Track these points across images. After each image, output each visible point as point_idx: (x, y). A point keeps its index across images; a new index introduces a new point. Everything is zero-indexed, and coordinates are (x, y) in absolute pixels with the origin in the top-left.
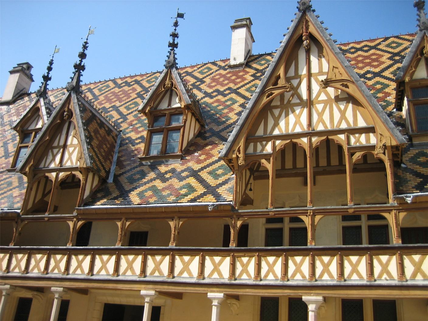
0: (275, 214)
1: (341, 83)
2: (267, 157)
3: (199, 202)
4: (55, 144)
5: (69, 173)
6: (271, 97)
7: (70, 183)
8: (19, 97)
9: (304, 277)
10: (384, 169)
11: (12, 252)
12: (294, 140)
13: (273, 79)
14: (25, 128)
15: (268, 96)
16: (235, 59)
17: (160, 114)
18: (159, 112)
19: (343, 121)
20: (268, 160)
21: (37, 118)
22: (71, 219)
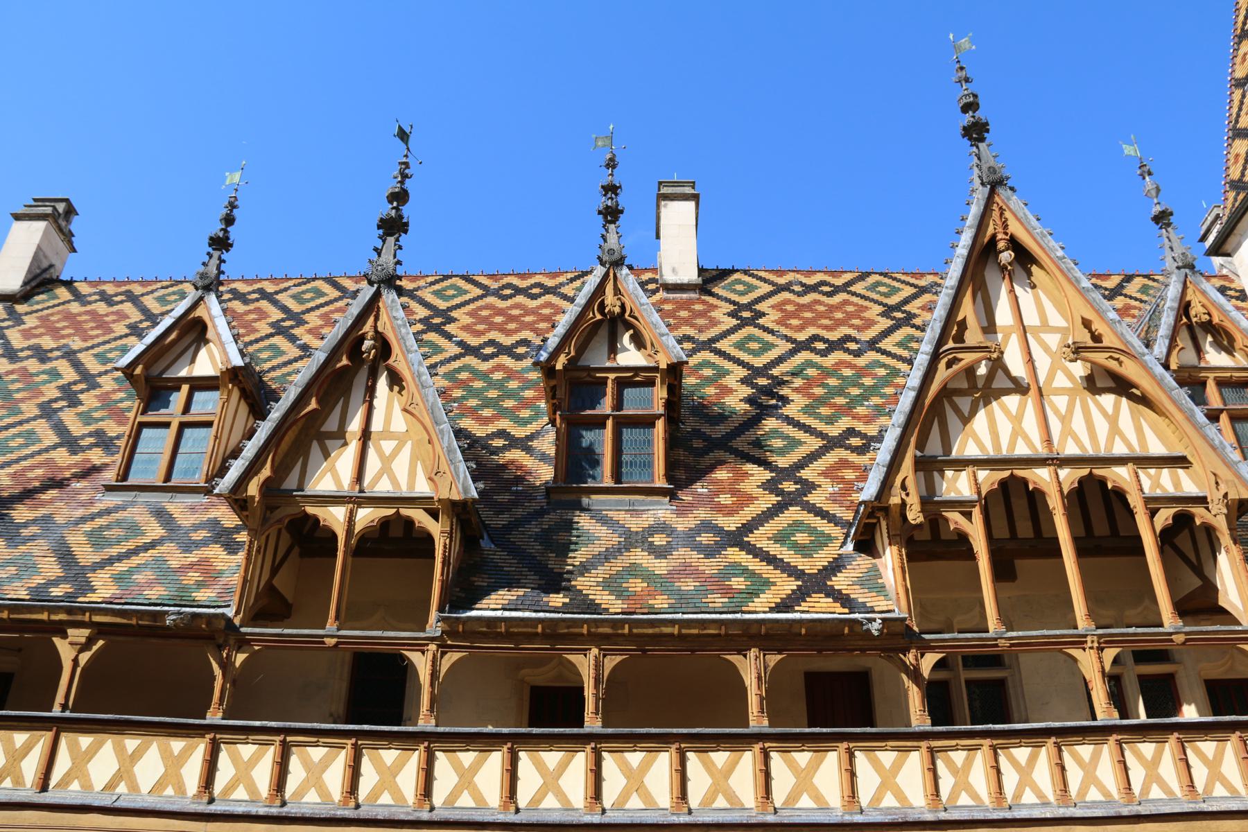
0: (1012, 645)
1: (1108, 355)
2: (963, 506)
3: (803, 612)
4: (331, 424)
5: (391, 512)
6: (955, 367)
7: (395, 540)
8: (38, 286)
9: (1106, 793)
10: (1058, 553)
11: (217, 737)
13: (953, 327)
14: (155, 371)
15: (949, 365)
16: (674, 270)
17: (588, 379)
18: (585, 374)
19: (1117, 438)
20: (968, 515)
21: (193, 348)
22: (420, 648)
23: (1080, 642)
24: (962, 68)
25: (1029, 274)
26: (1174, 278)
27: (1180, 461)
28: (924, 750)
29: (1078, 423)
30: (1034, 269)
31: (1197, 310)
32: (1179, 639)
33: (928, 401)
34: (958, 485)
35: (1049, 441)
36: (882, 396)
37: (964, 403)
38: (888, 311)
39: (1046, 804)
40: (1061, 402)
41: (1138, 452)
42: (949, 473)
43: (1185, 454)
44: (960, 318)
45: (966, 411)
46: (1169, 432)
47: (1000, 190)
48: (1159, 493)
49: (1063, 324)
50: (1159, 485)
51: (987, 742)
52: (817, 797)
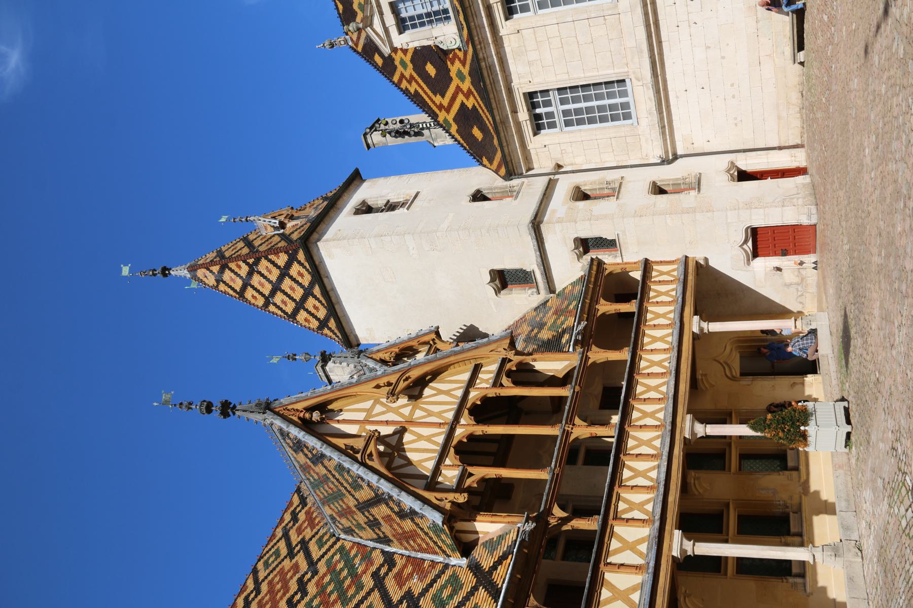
0: (560, 466)
2: (464, 475)
3: (503, 582)
12: (455, 442)
13: (349, 452)
20: (471, 475)
23: (568, 434)
24: (181, 404)
25: (332, 410)
26: (364, 361)
27: (477, 369)
28: (614, 523)
29: (436, 409)
30: (330, 407)
31: (386, 356)
32: (577, 388)
33: (390, 476)
34: (450, 474)
35: (440, 425)
36: (356, 556)
37: (398, 462)
38: (291, 554)
39: (659, 466)
40: (418, 413)
41: (464, 385)
42: (440, 479)
43: (473, 365)
44: (344, 447)
45: (403, 462)
46: (457, 368)
47: (273, 406)
48: (491, 381)
49: (371, 402)
50: (487, 380)
51: (616, 489)
52: (633, 589)
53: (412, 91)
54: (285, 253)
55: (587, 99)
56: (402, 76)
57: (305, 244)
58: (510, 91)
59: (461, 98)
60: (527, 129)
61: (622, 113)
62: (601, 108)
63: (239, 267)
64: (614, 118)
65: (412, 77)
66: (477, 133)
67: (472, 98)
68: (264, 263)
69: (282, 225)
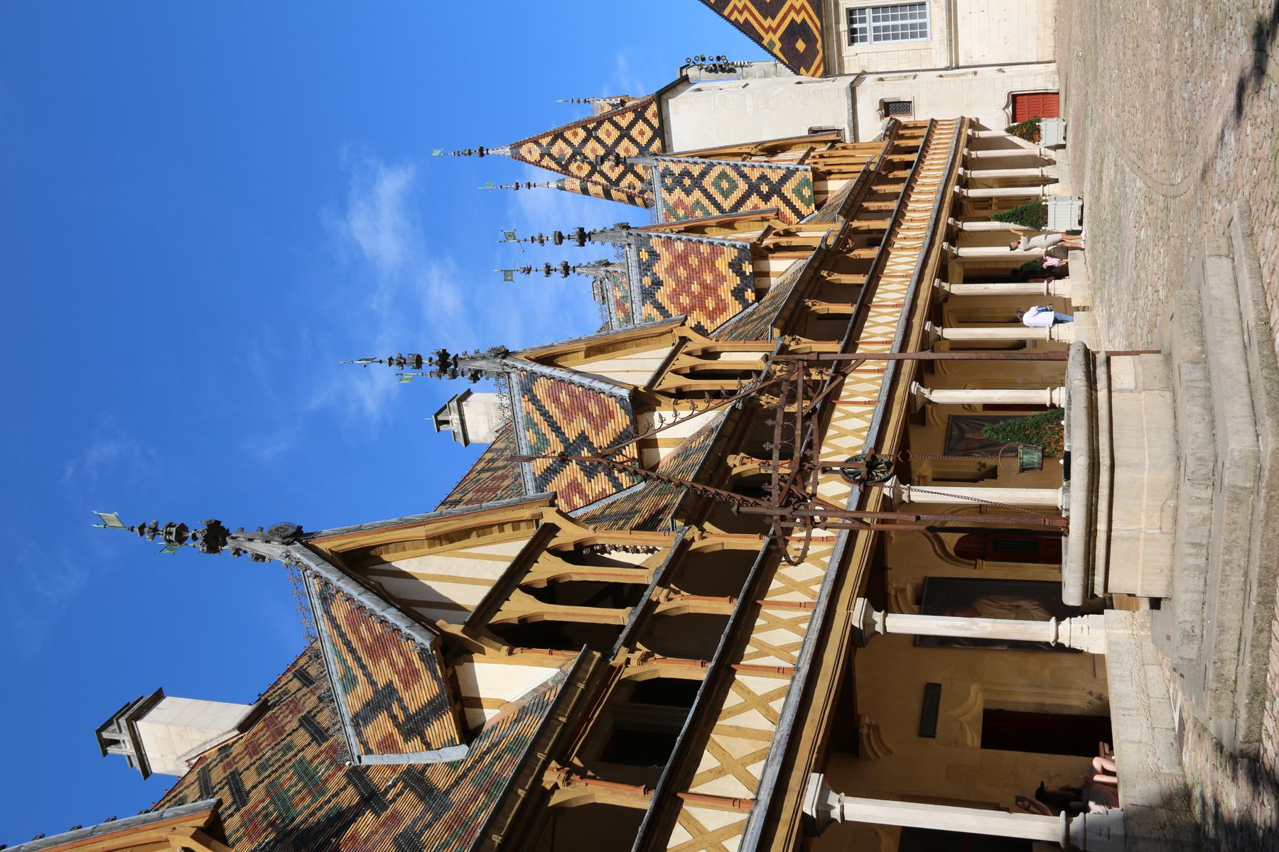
27: (812, 149)
53: (741, 20)
54: (634, 111)
55: (894, 18)
56: (735, 7)
57: (661, 97)
58: (837, 5)
59: (793, 14)
60: (845, 38)
61: (919, 32)
62: (904, 27)
63: (575, 134)
64: (913, 36)
65: (745, 7)
66: (801, 46)
67: (803, 14)
68: (607, 125)
69: (623, 103)
